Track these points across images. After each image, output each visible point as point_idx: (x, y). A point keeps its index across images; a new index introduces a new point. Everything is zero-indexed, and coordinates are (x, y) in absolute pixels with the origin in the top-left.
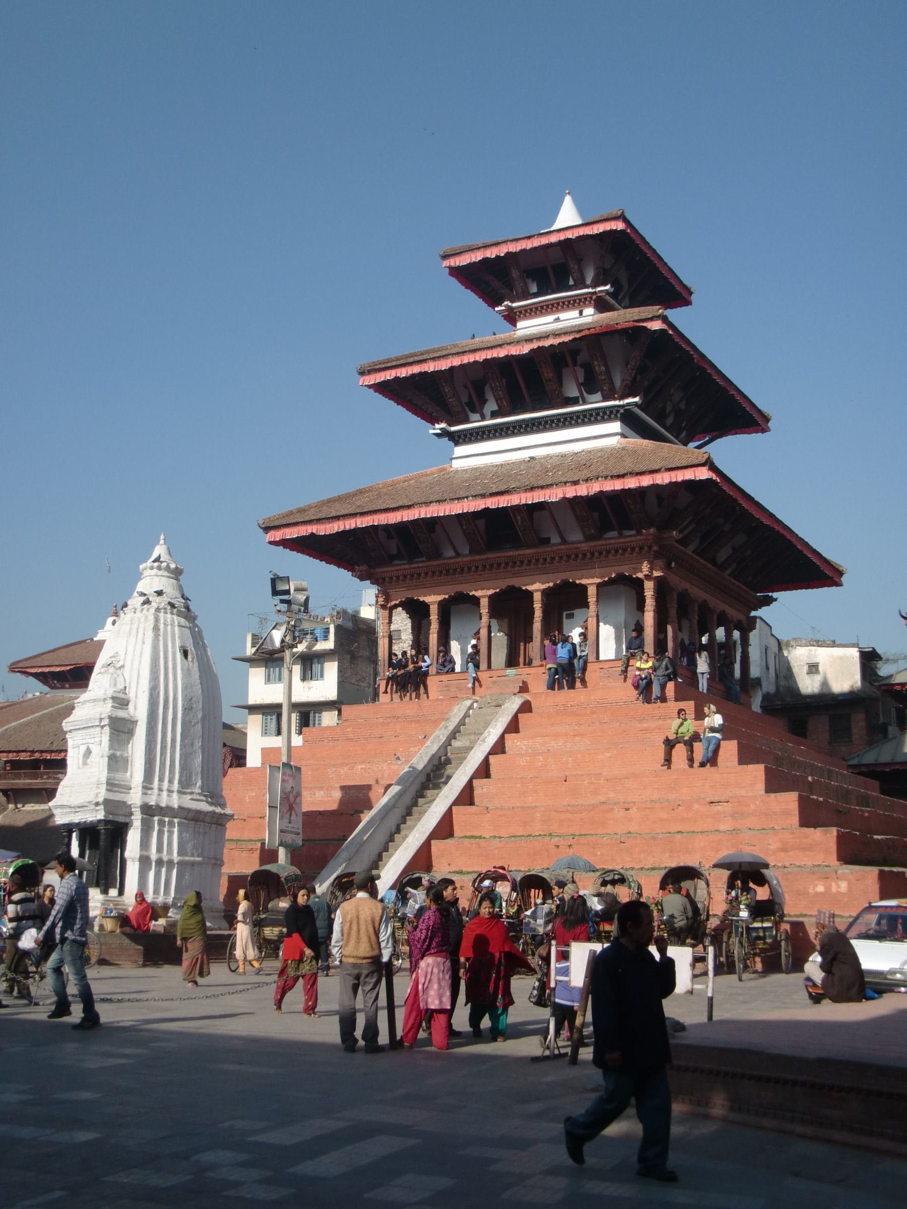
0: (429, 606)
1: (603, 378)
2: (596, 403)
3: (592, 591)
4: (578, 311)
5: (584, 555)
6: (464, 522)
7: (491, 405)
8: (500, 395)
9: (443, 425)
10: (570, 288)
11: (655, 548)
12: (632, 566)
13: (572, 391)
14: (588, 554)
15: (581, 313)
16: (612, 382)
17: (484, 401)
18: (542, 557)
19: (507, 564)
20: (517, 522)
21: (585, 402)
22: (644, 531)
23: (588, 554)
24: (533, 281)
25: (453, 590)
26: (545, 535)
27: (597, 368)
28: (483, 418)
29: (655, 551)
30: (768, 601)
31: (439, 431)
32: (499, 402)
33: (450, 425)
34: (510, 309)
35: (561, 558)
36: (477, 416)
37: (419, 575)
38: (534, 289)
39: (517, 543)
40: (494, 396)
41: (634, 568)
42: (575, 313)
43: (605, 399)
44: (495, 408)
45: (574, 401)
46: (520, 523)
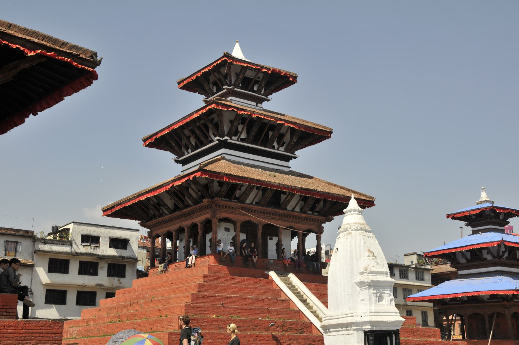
4: (256, 103)
10: (255, 92)
13: (275, 144)
21: (278, 149)
27: (293, 139)
28: (238, 140)
33: (227, 140)
38: (240, 85)
42: (255, 104)
43: (286, 151)
45: (273, 148)
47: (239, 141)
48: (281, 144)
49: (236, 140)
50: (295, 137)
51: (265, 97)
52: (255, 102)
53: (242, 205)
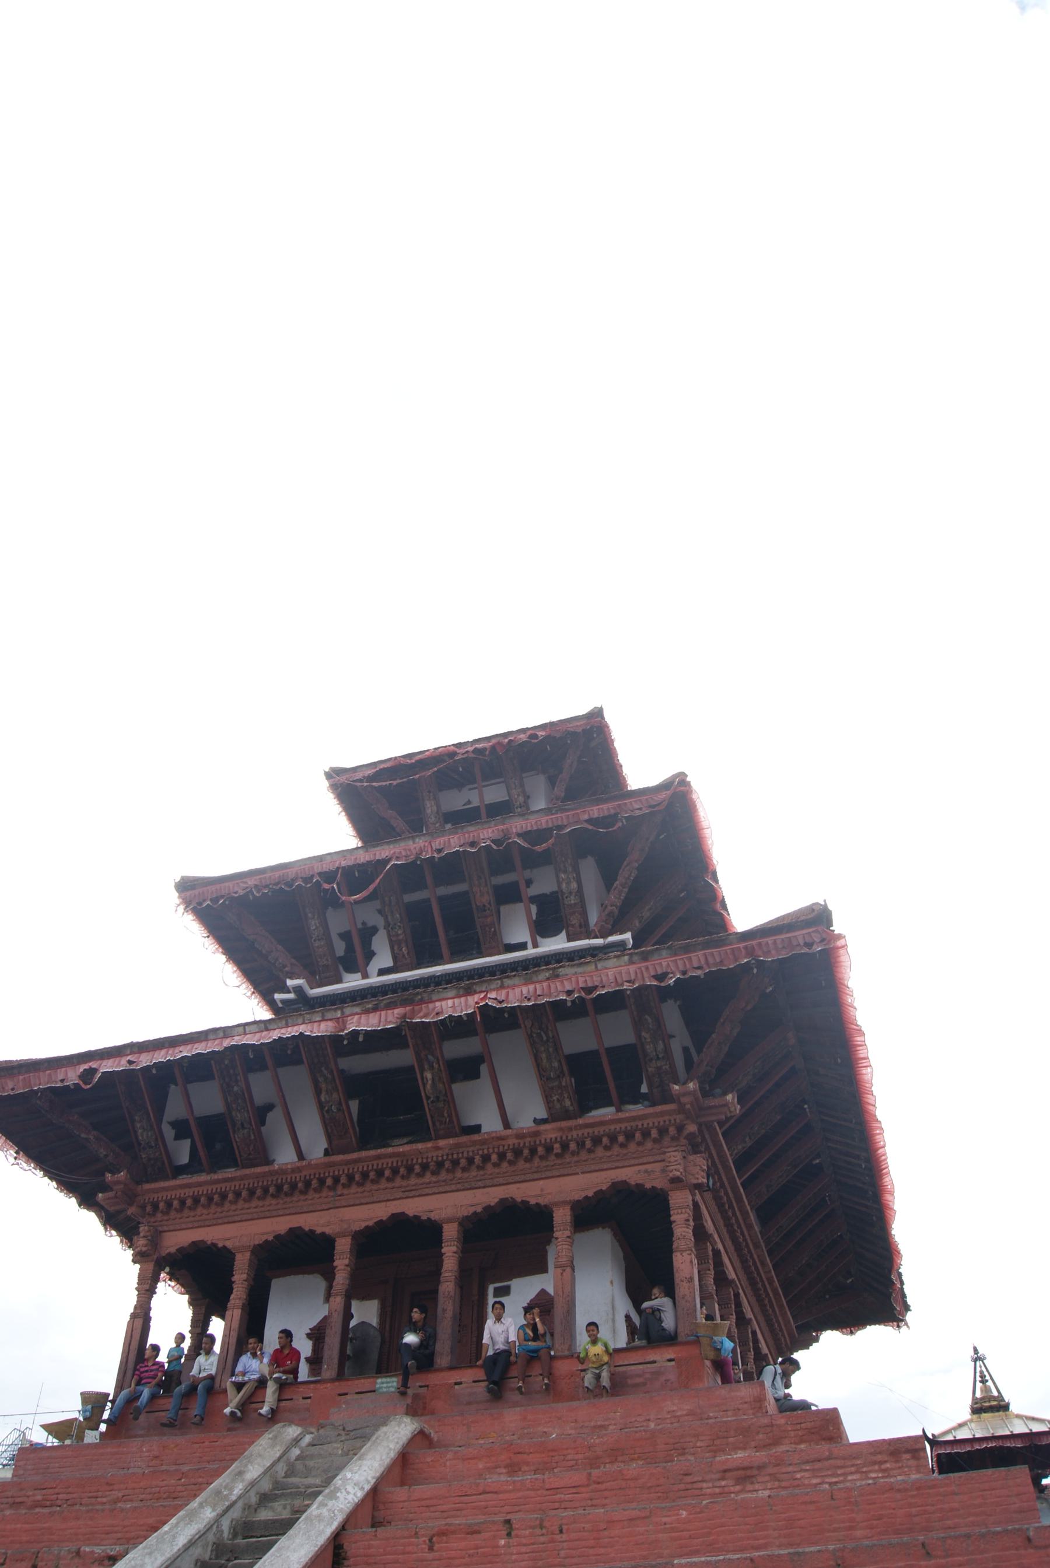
0: (234, 1254)
1: (572, 902)
3: (562, 1217)
5: (549, 1149)
6: (323, 1086)
7: (384, 958)
8: (398, 935)
11: (692, 1128)
12: (642, 1168)
13: (518, 930)
14: (557, 1146)
16: (584, 914)
17: (370, 955)
18: (465, 1155)
20: (424, 1085)
23: (557, 1146)
26: (473, 1122)
29: (691, 1137)
31: (291, 996)
32: (396, 948)
35: (502, 1156)
37: (224, 1196)
39: (419, 1131)
40: (389, 936)
41: (646, 1171)
44: (389, 963)
46: (428, 1087)
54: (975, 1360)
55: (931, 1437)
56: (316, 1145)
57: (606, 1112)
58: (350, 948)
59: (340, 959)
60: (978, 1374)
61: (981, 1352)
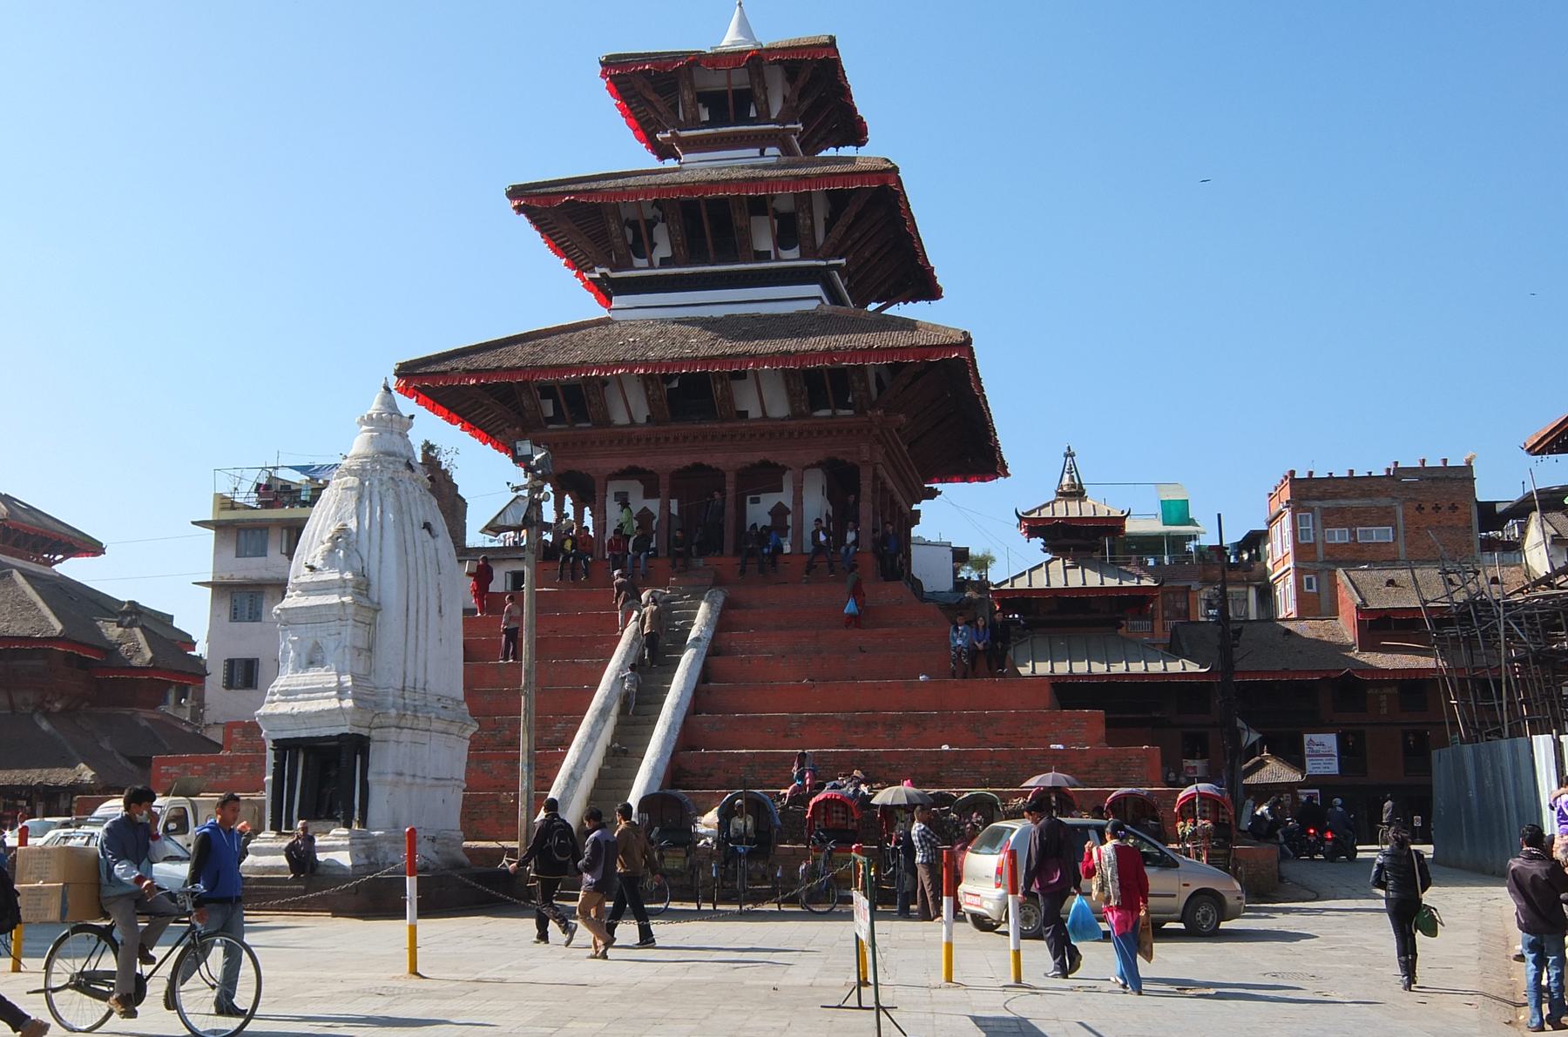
2: (791, 258)
7: (663, 250)
8: (676, 240)
9: (604, 270)
13: (764, 242)
14: (796, 433)
15: (762, 153)
17: (653, 245)
19: (695, 437)
20: (716, 392)
21: (778, 259)
22: (869, 412)
23: (796, 433)
24: (704, 106)
25: (624, 463)
27: (801, 221)
28: (651, 266)
30: (933, 494)
31: (598, 276)
33: (612, 271)
34: (675, 137)
36: (644, 262)
38: (705, 116)
42: (756, 152)
43: (803, 257)
44: (668, 253)
45: (764, 256)
46: (719, 392)
47: (654, 268)
48: (784, 241)
49: (647, 265)
50: (801, 215)
51: (777, 127)
52: (756, 148)
53: (607, 430)
54: (1066, 456)
55: (1020, 514)
56: (642, 414)
57: (826, 413)
58: (637, 237)
59: (631, 246)
60: (1067, 467)
61: (1072, 450)
